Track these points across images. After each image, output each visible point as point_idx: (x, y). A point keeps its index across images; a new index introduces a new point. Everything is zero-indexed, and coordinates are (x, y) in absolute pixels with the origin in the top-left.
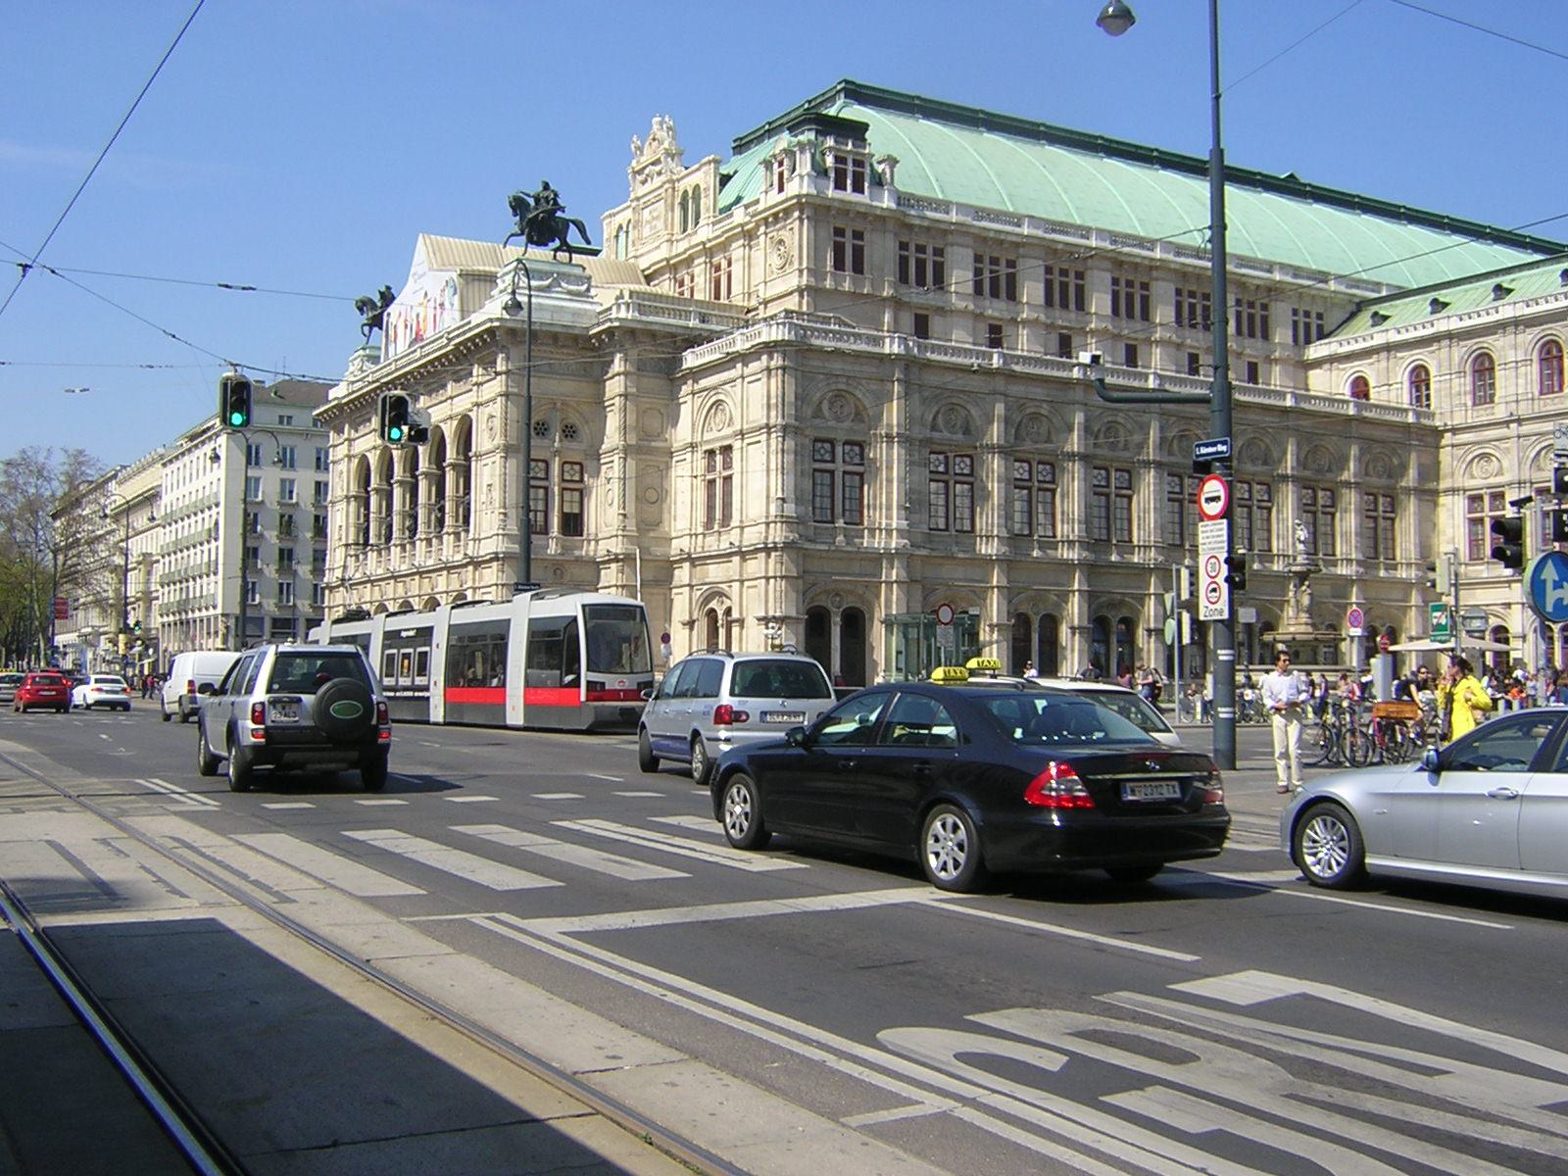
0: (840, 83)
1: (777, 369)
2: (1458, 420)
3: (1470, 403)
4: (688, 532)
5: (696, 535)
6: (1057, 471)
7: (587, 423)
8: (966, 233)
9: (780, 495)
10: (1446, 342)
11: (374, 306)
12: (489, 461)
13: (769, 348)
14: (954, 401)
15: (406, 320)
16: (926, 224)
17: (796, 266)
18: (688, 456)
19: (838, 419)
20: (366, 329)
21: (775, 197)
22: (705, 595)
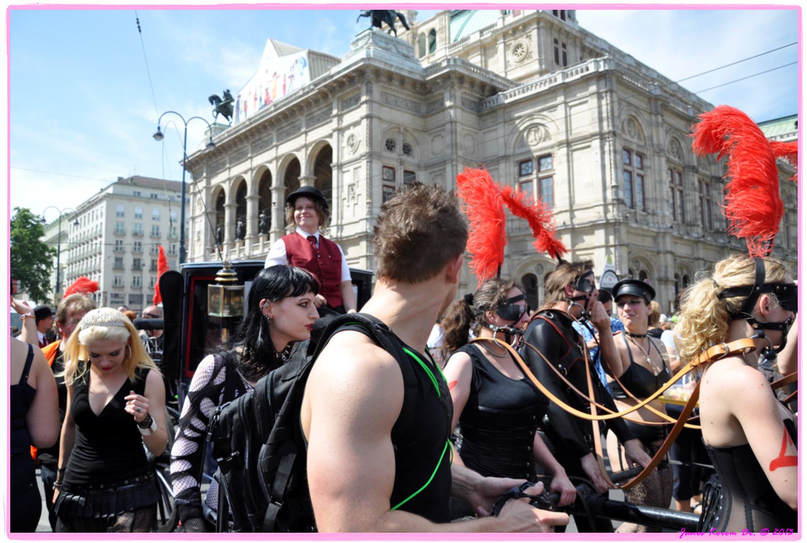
1: (606, 92)
6: (710, 188)
7: (418, 144)
9: (614, 184)
11: (220, 101)
12: (351, 168)
13: (599, 76)
14: (675, 135)
15: (256, 95)
16: (591, 47)
17: (535, 56)
18: (502, 166)
19: (630, 135)
20: (215, 113)
21: (510, 19)
22: (523, 263)
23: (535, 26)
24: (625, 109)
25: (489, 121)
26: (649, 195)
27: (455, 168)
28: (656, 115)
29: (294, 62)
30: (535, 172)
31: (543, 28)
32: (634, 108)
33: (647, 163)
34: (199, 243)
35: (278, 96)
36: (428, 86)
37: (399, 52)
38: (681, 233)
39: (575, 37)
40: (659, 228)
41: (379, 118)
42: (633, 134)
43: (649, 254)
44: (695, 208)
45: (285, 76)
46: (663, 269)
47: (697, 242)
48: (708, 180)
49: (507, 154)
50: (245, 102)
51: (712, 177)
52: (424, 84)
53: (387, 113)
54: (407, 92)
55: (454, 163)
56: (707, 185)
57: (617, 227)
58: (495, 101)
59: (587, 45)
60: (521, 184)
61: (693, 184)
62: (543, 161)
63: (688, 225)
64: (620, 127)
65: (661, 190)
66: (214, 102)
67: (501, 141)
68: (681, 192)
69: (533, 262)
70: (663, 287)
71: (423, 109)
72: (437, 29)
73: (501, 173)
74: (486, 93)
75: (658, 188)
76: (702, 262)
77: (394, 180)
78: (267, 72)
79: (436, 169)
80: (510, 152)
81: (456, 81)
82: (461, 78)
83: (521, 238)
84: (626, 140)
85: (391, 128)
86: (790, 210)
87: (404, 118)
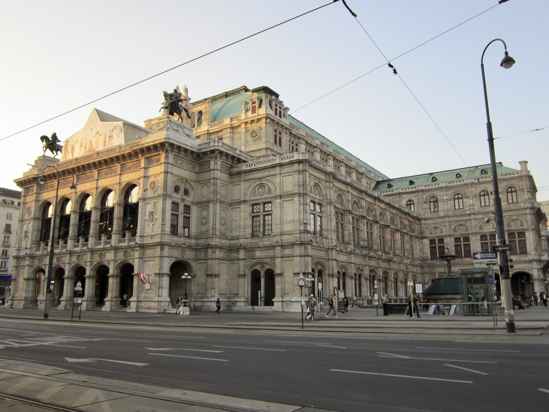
0: (242, 87)
2: (426, 216)
3: (429, 212)
4: (243, 237)
5: (247, 238)
7: (193, 189)
8: (304, 140)
10: (420, 193)
12: (152, 202)
14: (340, 193)
16: (296, 134)
17: (264, 139)
18: (242, 206)
19: (315, 194)
20: (44, 148)
22: (253, 264)
23: (264, 120)
24: (313, 180)
25: (236, 179)
26: (324, 227)
27: (215, 205)
28: (329, 182)
29: (113, 128)
30: (262, 210)
31: (269, 123)
32: (318, 179)
33: (323, 209)
34: (26, 239)
35: (100, 148)
36: (201, 155)
37: (184, 132)
38: (342, 248)
39: (286, 128)
40: (329, 246)
41: (172, 174)
42: (316, 193)
43: (323, 260)
44: (350, 234)
45: (105, 135)
46: (331, 269)
47: (350, 253)
48: (358, 217)
49: (246, 200)
50: (73, 147)
51: (360, 216)
52: (198, 155)
53: (175, 171)
54: (188, 158)
55: (215, 203)
56: (357, 220)
57: (306, 246)
58: (240, 168)
59: (293, 133)
60: (253, 217)
61: (349, 220)
62: (266, 205)
63: (346, 244)
64: (310, 190)
65: (331, 225)
66: (44, 140)
67: (243, 192)
68: (342, 224)
69: (258, 263)
70: (331, 279)
71: (197, 169)
72: (203, 112)
73: (242, 210)
74: (235, 162)
75: (329, 224)
76: (353, 265)
77: (178, 211)
78: (92, 130)
79: (203, 205)
80: (247, 198)
81: (218, 156)
82: (221, 152)
83: (252, 249)
84: (313, 197)
85: (178, 180)
86: (405, 233)
87: (185, 173)
